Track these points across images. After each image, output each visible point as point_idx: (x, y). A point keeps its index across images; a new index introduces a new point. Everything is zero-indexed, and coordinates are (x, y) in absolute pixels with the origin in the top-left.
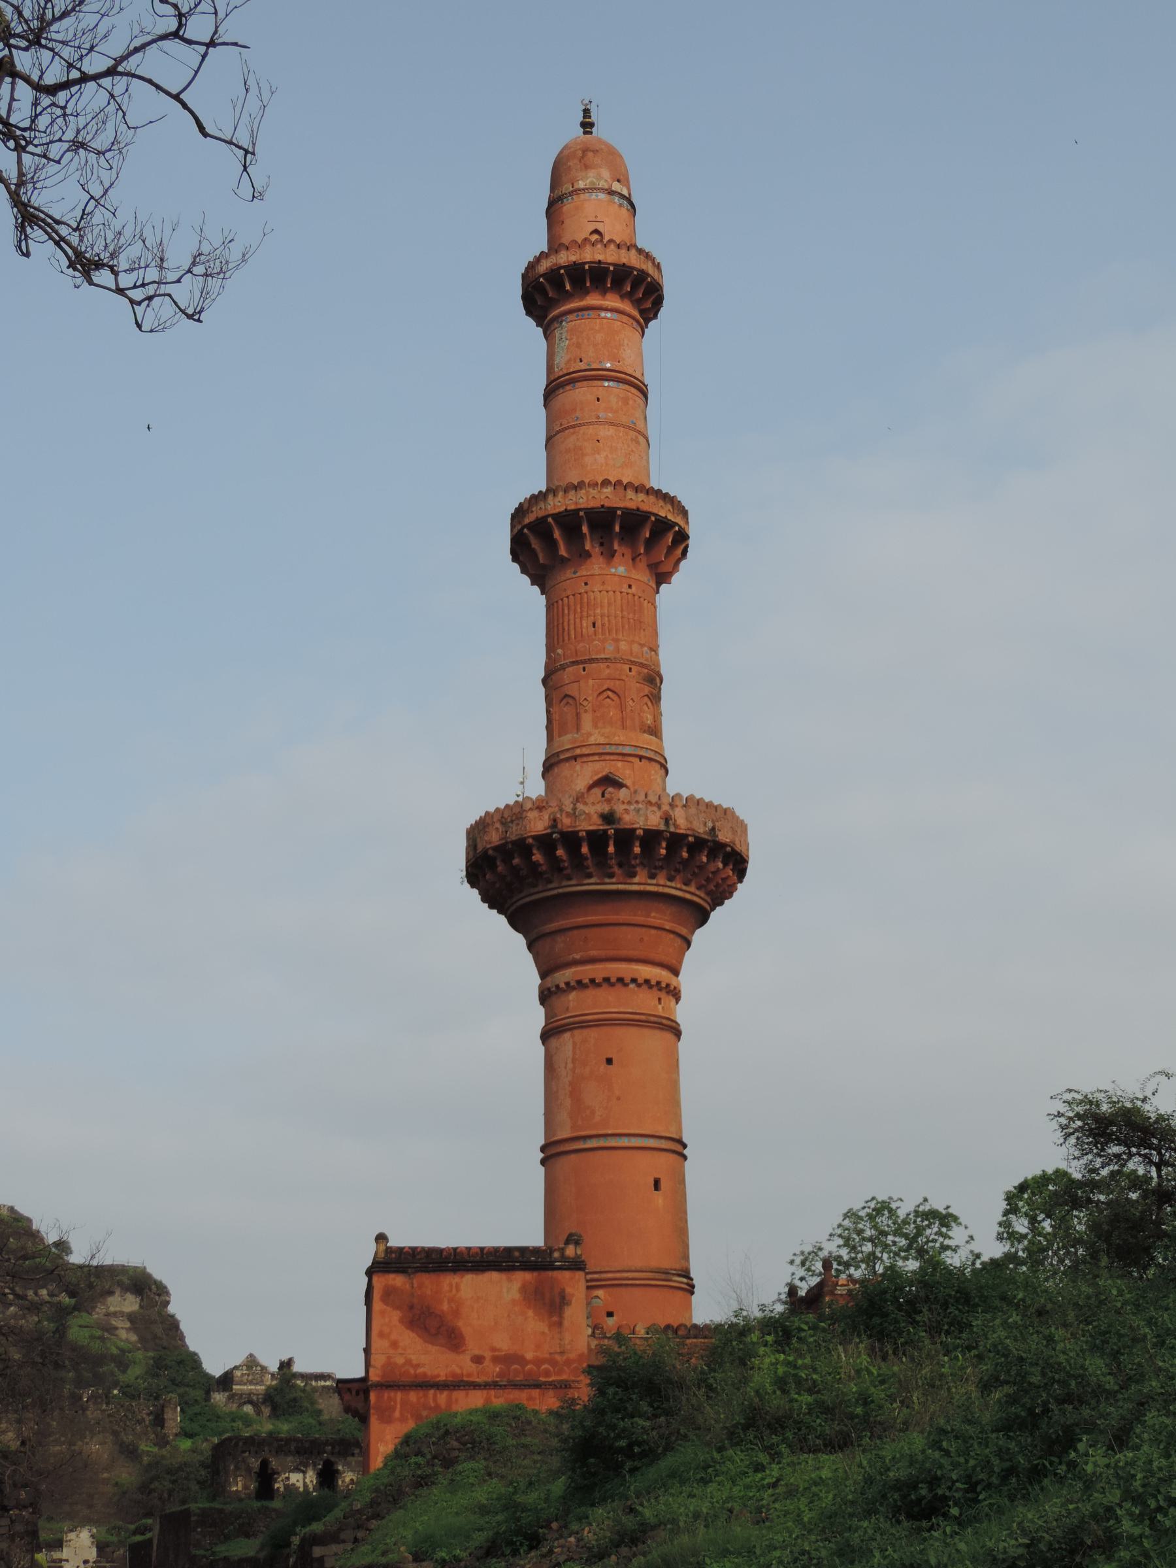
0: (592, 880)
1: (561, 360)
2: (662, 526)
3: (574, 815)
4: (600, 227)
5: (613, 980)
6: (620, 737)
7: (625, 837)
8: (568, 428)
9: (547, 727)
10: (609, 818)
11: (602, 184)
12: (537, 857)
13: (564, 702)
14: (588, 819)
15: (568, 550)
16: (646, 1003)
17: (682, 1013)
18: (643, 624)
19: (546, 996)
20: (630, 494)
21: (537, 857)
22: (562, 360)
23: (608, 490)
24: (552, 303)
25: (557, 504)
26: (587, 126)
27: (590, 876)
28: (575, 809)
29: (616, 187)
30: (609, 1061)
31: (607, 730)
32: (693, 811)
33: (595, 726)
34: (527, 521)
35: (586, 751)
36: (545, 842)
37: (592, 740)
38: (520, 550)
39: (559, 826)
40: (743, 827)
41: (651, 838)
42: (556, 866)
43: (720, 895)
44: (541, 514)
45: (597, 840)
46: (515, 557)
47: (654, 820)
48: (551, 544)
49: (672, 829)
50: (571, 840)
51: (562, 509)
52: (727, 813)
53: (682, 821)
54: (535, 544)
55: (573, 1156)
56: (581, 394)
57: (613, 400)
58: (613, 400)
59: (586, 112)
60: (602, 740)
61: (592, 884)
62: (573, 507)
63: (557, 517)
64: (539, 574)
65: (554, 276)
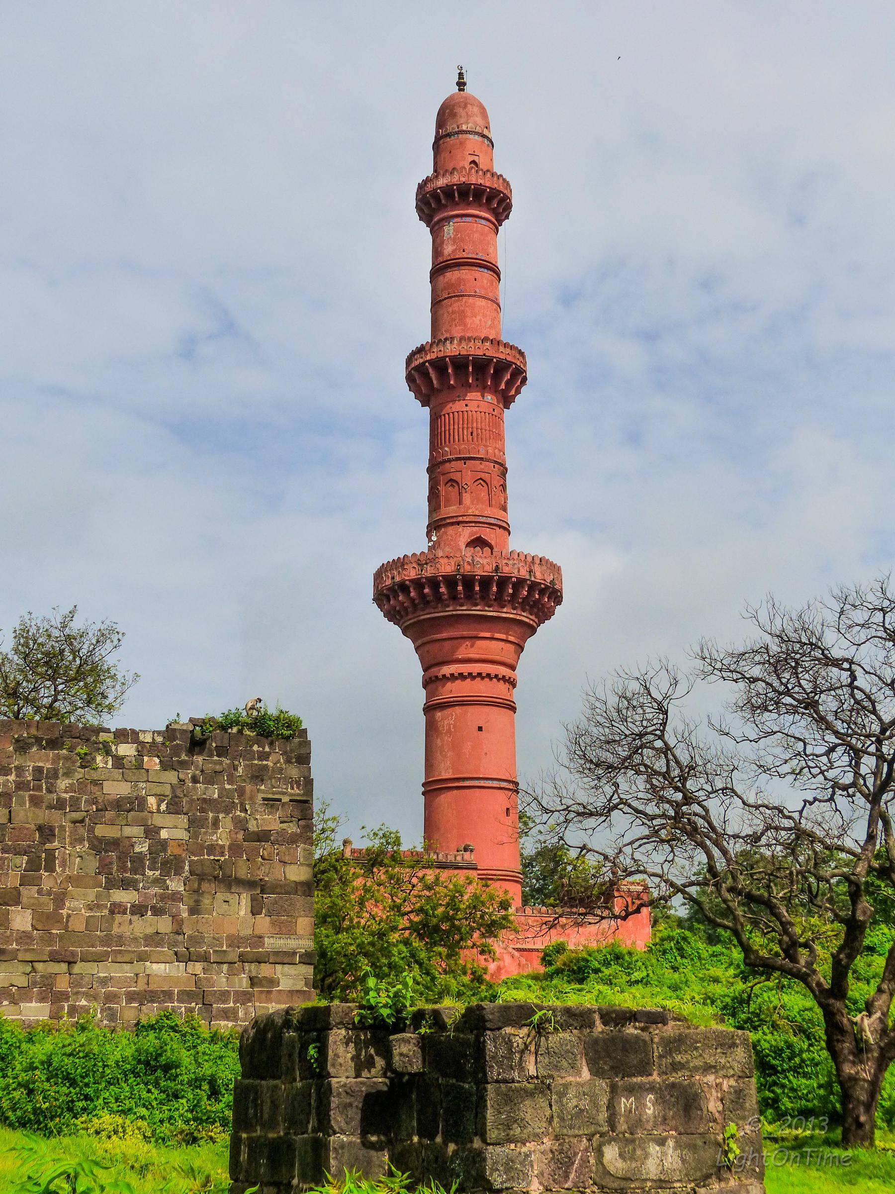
0: (478, 608)
1: (448, 250)
3: (472, 564)
4: (476, 159)
5: (484, 675)
6: (488, 512)
8: (452, 297)
9: (430, 499)
11: (478, 129)
12: (443, 590)
13: (450, 484)
15: (455, 381)
16: (499, 690)
20: (502, 349)
21: (443, 590)
22: (448, 250)
23: (488, 344)
24: (441, 207)
25: (451, 349)
26: (461, 85)
27: (476, 605)
28: (473, 560)
29: (486, 132)
30: (480, 729)
31: (480, 506)
32: (544, 568)
33: (472, 502)
34: (428, 358)
35: (465, 519)
36: (451, 581)
37: (470, 512)
39: (462, 571)
44: (441, 355)
45: (486, 582)
46: (410, 379)
47: (524, 574)
49: (533, 579)
50: (468, 581)
51: (457, 353)
54: (433, 374)
55: (455, 792)
56: (464, 273)
57: (485, 282)
58: (485, 282)
59: (461, 75)
60: (477, 513)
62: (465, 353)
63: (453, 359)
65: (448, 191)
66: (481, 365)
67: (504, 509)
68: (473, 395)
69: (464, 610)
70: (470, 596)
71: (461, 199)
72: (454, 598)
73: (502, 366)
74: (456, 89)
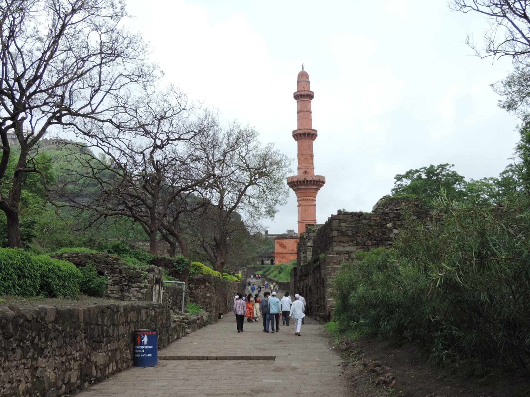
2: (313, 134)
7: (307, 181)
10: (305, 179)
14: (302, 179)
16: (311, 202)
17: (316, 203)
18: (311, 148)
19: (298, 201)
26: (303, 68)
29: (307, 80)
36: (297, 182)
38: (293, 136)
40: (324, 177)
41: (311, 181)
42: (298, 185)
43: (322, 186)
45: (304, 182)
47: (311, 179)
48: (298, 138)
50: (300, 182)
52: (321, 176)
53: (315, 179)
61: (303, 187)
64: (296, 140)
65: (298, 96)
66: (304, 134)
67: (312, 164)
68: (304, 140)
69: (300, 187)
70: (301, 184)
71: (304, 96)
72: (298, 185)
73: (309, 134)
74: (302, 70)
